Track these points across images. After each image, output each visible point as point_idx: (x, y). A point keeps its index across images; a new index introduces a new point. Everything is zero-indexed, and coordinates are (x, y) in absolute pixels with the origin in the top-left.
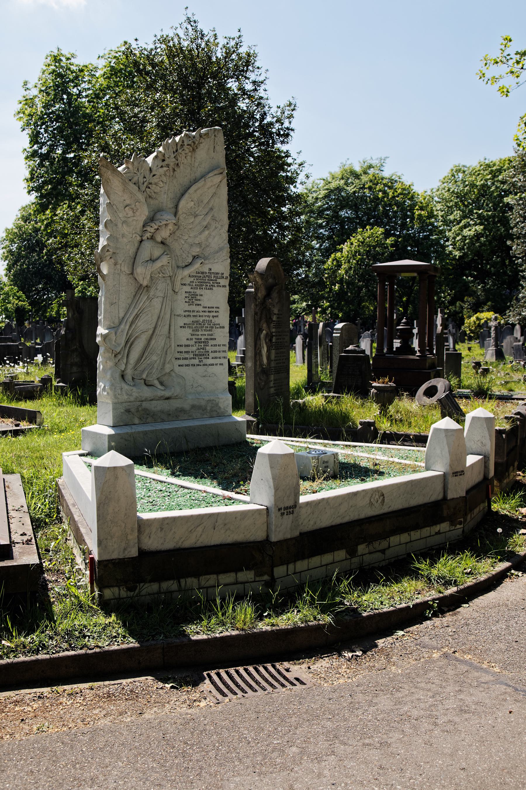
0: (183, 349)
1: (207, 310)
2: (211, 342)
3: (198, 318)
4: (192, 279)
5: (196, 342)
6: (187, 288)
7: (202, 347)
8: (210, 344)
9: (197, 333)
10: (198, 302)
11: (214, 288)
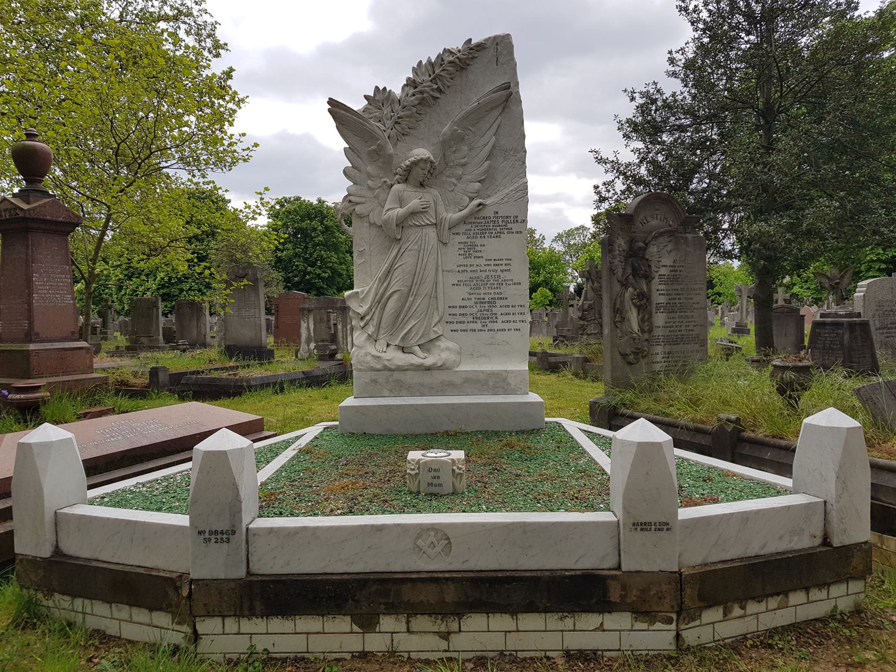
0: (457, 311)
1: (492, 263)
2: (499, 303)
3: (478, 274)
4: (469, 227)
6: (463, 238)
7: (487, 308)
8: (498, 305)
9: (477, 291)
10: (478, 254)
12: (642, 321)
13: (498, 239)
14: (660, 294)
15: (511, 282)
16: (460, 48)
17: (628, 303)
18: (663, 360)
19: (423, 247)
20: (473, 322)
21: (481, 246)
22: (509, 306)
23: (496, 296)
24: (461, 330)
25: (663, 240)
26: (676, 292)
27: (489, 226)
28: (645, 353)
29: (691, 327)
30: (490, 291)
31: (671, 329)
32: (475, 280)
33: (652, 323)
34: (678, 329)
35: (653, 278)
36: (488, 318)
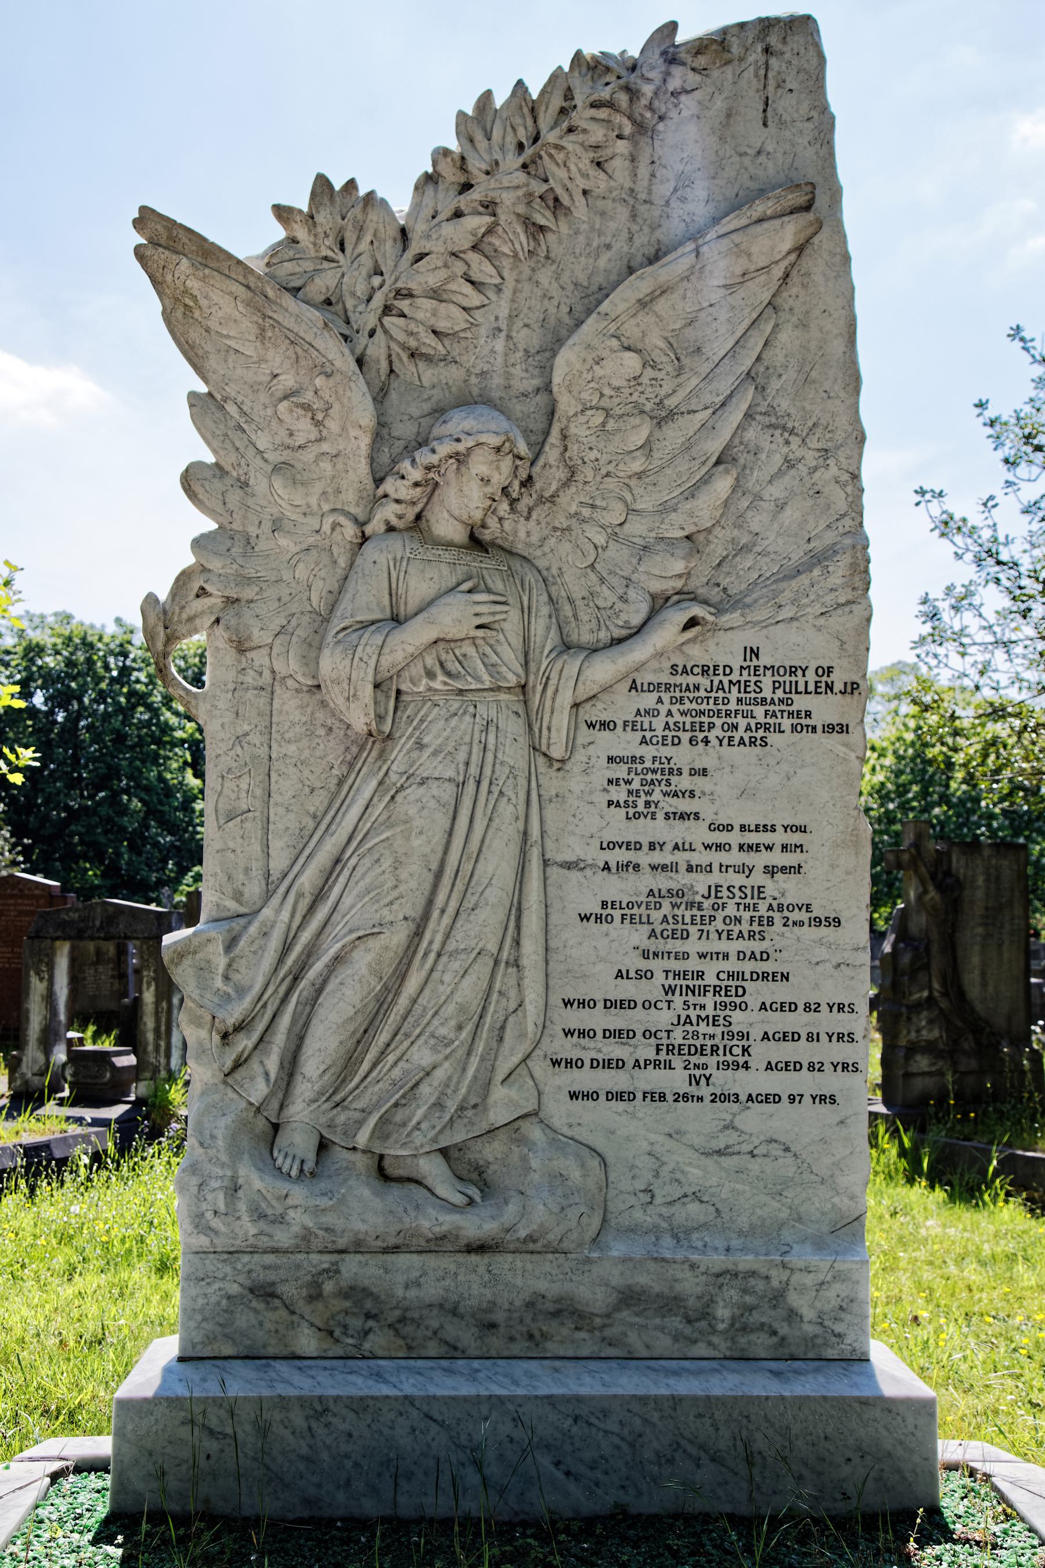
3: (683, 879)
13: (758, 750)
15: (804, 916)
16: (635, 52)
19: (474, 770)
20: (657, 1064)
21: (693, 772)
22: (793, 1007)
23: (748, 967)
24: (611, 1096)
27: (726, 701)
30: (723, 946)
32: (666, 904)
36: (714, 1050)
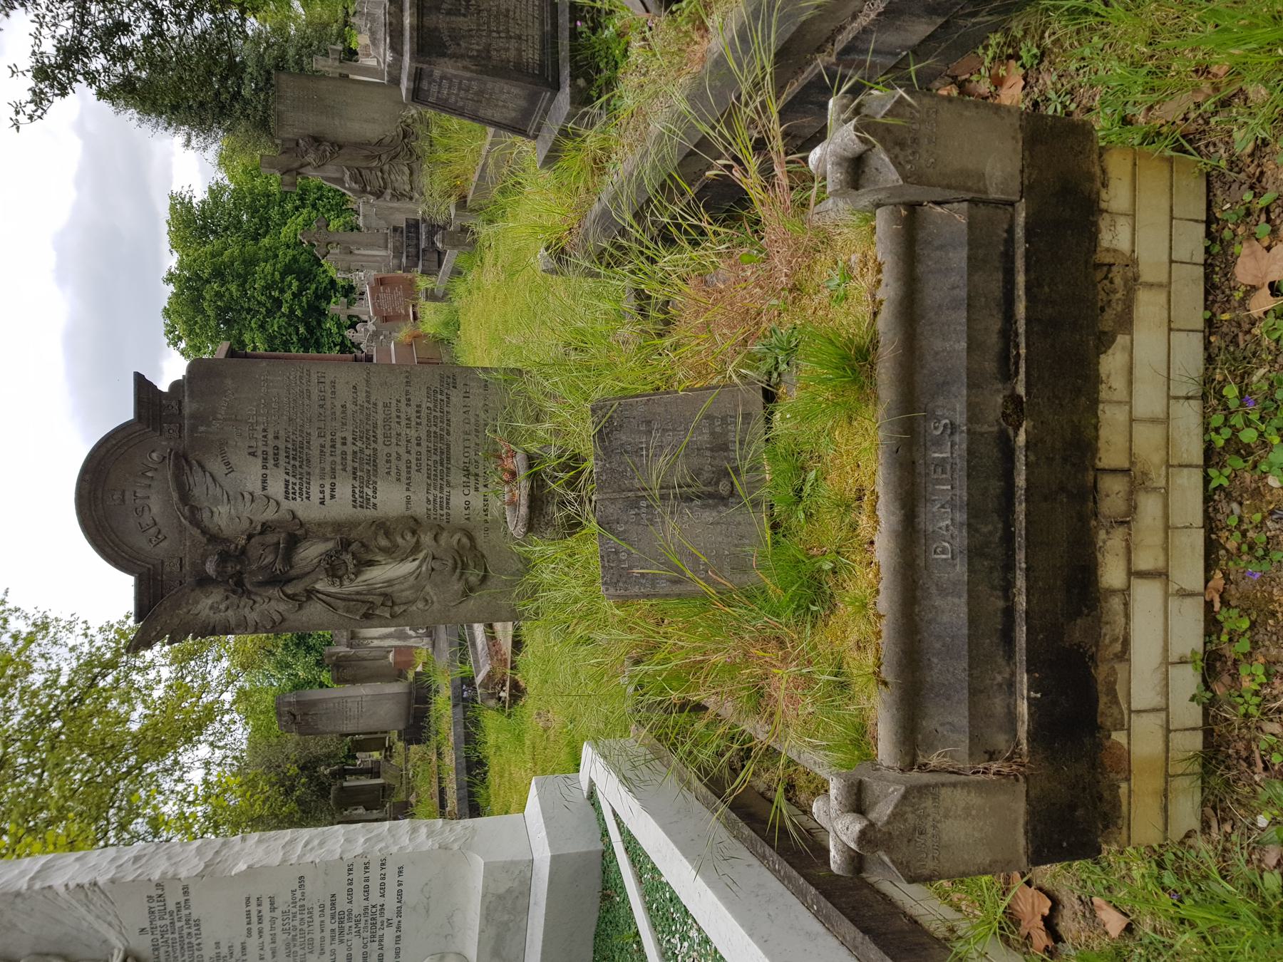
1: (255, 927)
5: (341, 941)
7: (353, 924)
9: (317, 942)
11: (194, 917)
12: (392, 552)
14: (333, 497)
17: (349, 588)
18: (482, 489)
25: (200, 487)
26: (328, 450)
28: (465, 540)
29: (412, 412)
31: (414, 467)
33: (399, 519)
34: (414, 449)
35: (294, 517)
